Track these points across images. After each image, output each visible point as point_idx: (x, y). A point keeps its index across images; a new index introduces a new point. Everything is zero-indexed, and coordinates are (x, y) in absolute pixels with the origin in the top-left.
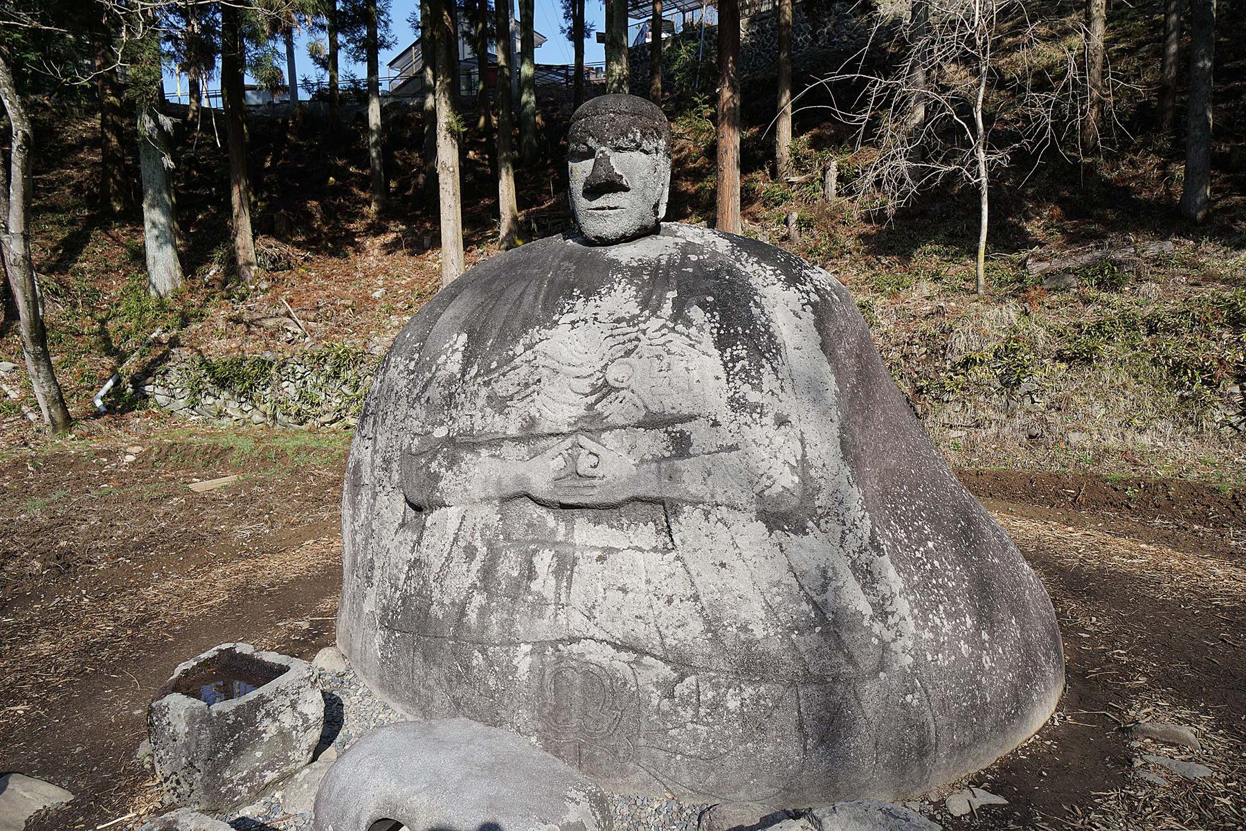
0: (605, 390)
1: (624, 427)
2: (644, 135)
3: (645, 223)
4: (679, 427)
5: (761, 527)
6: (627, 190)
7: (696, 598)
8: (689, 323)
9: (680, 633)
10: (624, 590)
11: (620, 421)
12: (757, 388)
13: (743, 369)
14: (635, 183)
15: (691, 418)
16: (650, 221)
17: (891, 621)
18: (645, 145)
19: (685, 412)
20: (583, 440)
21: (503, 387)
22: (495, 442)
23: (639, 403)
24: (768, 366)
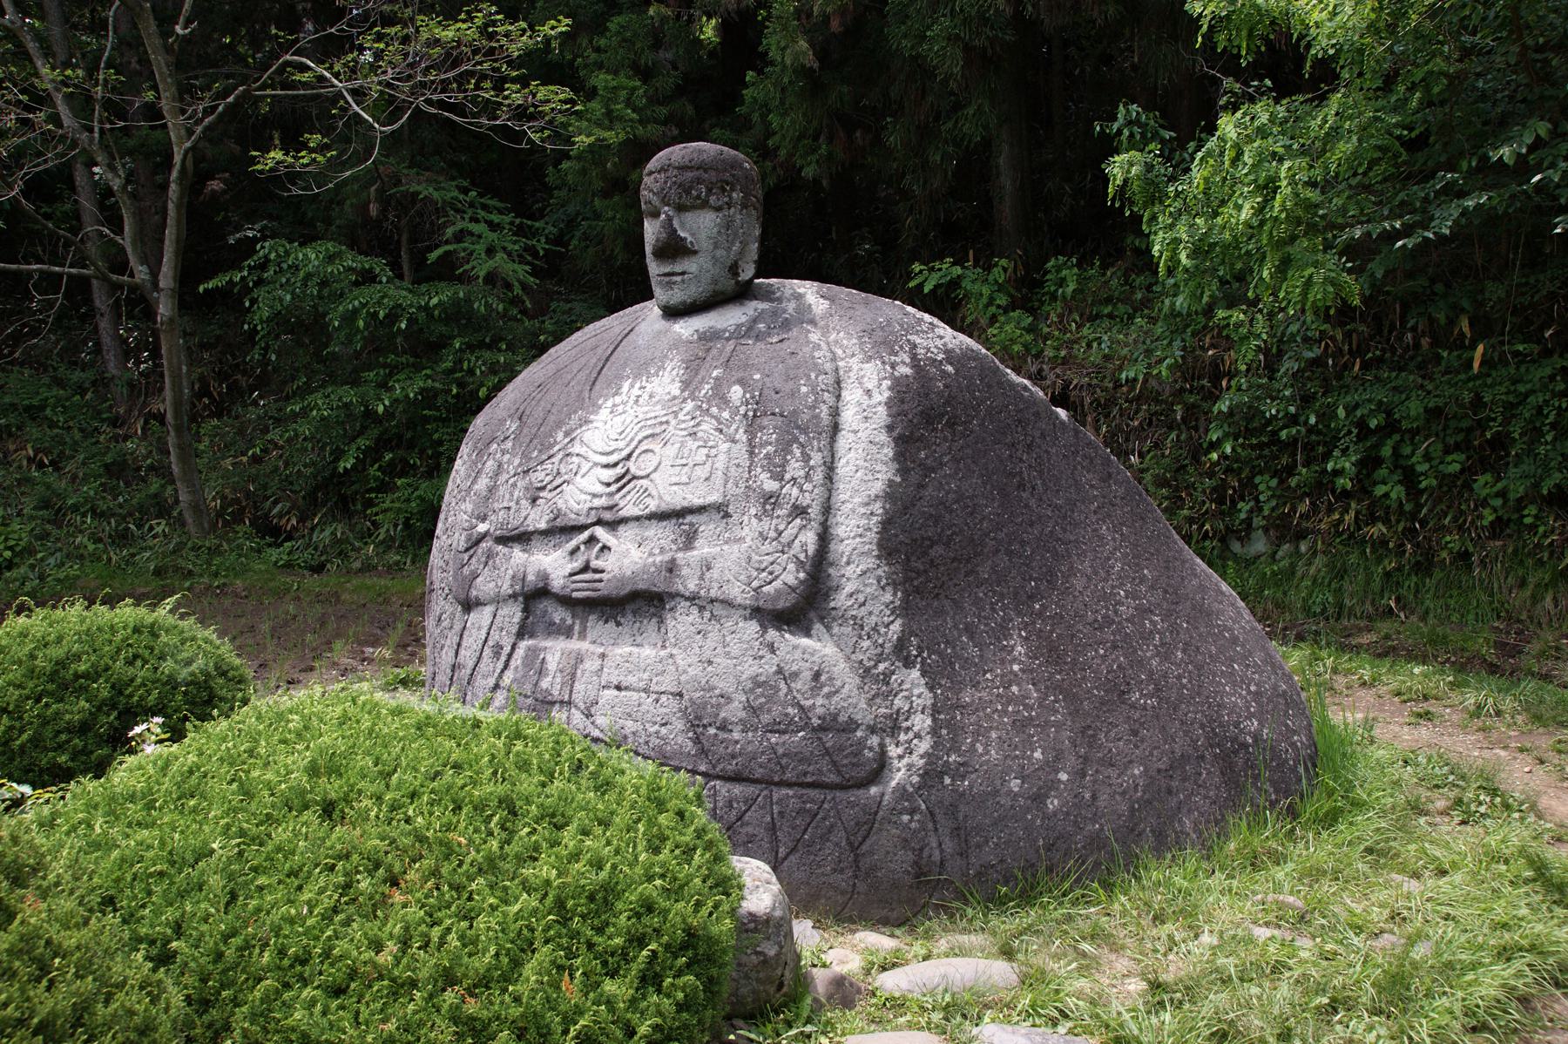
1: (637, 518)
2: (709, 191)
3: (719, 287)
4: (689, 519)
5: (753, 627)
6: (695, 252)
7: (680, 695)
9: (664, 731)
10: (618, 688)
11: (636, 512)
12: (778, 477)
13: (768, 456)
14: (704, 244)
15: (701, 510)
16: (728, 285)
17: (902, 737)
18: (712, 199)
19: (698, 502)
20: (600, 532)
21: (539, 476)
23: (654, 493)
24: (797, 452)
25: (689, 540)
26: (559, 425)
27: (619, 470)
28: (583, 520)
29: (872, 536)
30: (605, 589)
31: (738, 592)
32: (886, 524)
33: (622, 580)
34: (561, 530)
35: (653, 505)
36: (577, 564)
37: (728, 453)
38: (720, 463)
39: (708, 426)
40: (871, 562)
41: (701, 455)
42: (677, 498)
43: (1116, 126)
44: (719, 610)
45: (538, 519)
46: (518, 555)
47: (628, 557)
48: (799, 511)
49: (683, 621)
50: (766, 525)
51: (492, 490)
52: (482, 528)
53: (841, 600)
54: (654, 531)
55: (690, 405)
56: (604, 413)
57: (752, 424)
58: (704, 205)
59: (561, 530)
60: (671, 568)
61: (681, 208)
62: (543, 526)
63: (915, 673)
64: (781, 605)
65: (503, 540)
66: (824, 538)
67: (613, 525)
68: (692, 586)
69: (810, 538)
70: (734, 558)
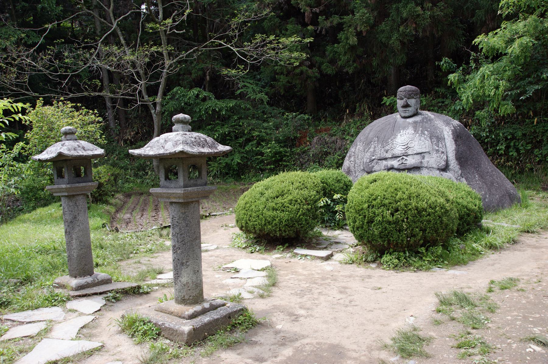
0: (408, 148)
5: (438, 171)
8: (424, 134)
12: (438, 147)
15: (425, 152)
19: (424, 151)
20: (404, 157)
21: (387, 148)
22: (385, 159)
25: (423, 158)
26: (389, 139)
27: (406, 146)
28: (400, 155)
29: (454, 156)
30: (407, 167)
31: (434, 166)
32: (456, 154)
33: (411, 165)
34: (395, 157)
35: (415, 152)
36: (400, 163)
37: (428, 143)
38: (427, 144)
39: (422, 138)
40: (455, 161)
41: (423, 143)
42: (420, 151)
43: (442, 63)
44: (431, 169)
45: (389, 155)
46: (384, 162)
47: (411, 161)
48: (443, 152)
49: (424, 172)
50: (438, 155)
51: (374, 151)
52: (373, 158)
53: (451, 167)
54: (416, 156)
55: (418, 135)
56: (399, 136)
57: (431, 138)
58: (413, 98)
59: (395, 157)
60: (421, 162)
61: (408, 98)
62: (390, 156)
63: (464, 179)
64: (443, 168)
65: (379, 160)
66: (447, 157)
67: (407, 156)
68: (426, 165)
69: (445, 157)
70: (433, 160)
